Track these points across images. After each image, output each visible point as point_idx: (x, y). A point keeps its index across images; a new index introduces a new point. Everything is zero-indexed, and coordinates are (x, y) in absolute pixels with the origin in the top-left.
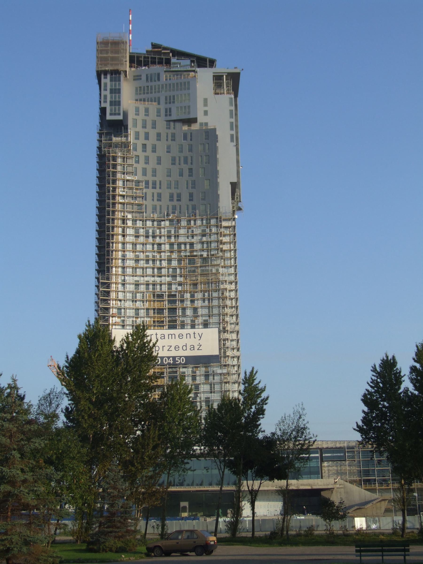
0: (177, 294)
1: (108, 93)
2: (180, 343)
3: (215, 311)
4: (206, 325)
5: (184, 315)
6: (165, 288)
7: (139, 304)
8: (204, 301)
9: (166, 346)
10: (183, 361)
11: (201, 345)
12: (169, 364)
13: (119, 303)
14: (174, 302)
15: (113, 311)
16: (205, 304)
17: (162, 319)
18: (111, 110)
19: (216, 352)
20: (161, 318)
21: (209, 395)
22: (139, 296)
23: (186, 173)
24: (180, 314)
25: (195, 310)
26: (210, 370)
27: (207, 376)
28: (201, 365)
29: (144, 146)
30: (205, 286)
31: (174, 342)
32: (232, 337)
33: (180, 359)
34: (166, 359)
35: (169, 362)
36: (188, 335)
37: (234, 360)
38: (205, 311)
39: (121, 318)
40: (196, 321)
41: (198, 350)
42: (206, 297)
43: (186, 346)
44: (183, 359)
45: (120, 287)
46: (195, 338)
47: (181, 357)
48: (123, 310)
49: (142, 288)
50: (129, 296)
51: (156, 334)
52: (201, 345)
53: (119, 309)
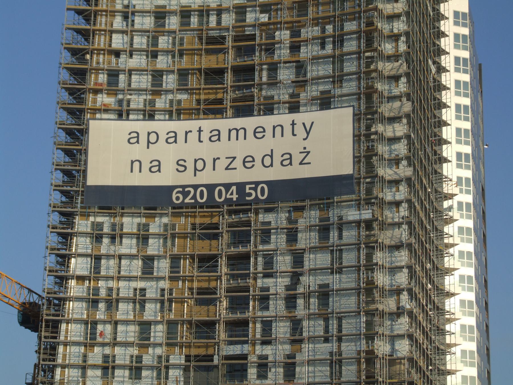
0: (258, 33)
2: (257, 148)
3: (350, 67)
4: (325, 102)
5: (273, 83)
6: (228, 19)
7: (162, 62)
8: (323, 46)
9: (223, 159)
10: (263, 194)
11: (308, 152)
12: (229, 202)
13: (114, 59)
14: (250, 51)
15: (97, 78)
16: (324, 52)
17: (220, 96)
19: (347, 168)
20: (216, 93)
22: (164, 42)
24: (264, 79)
25: (300, 67)
26: (333, 215)
27: (324, 230)
28: (308, 203)
30: (326, 7)
31: (240, 148)
32: (394, 131)
33: (255, 189)
34: (220, 191)
35: (228, 196)
36: (278, 130)
37: (398, 190)
38: (325, 69)
39: (116, 94)
40: (303, 95)
41: (301, 163)
42: (327, 33)
43: (271, 157)
44: (263, 189)
45: (118, 23)
46: (294, 135)
47: (257, 183)
48: (122, 77)
49: (173, 22)
50: (140, 42)
51: (200, 131)
52: (308, 152)
53: (113, 75)
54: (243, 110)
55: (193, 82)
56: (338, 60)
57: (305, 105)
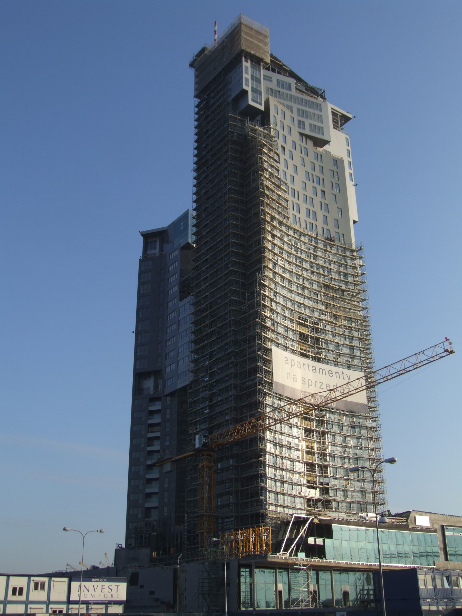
1: (249, 77)
18: (253, 96)
21: (357, 452)
23: (319, 193)
29: (283, 148)
54: (319, 360)
55: (298, 337)
56: (352, 348)
57: (342, 365)
